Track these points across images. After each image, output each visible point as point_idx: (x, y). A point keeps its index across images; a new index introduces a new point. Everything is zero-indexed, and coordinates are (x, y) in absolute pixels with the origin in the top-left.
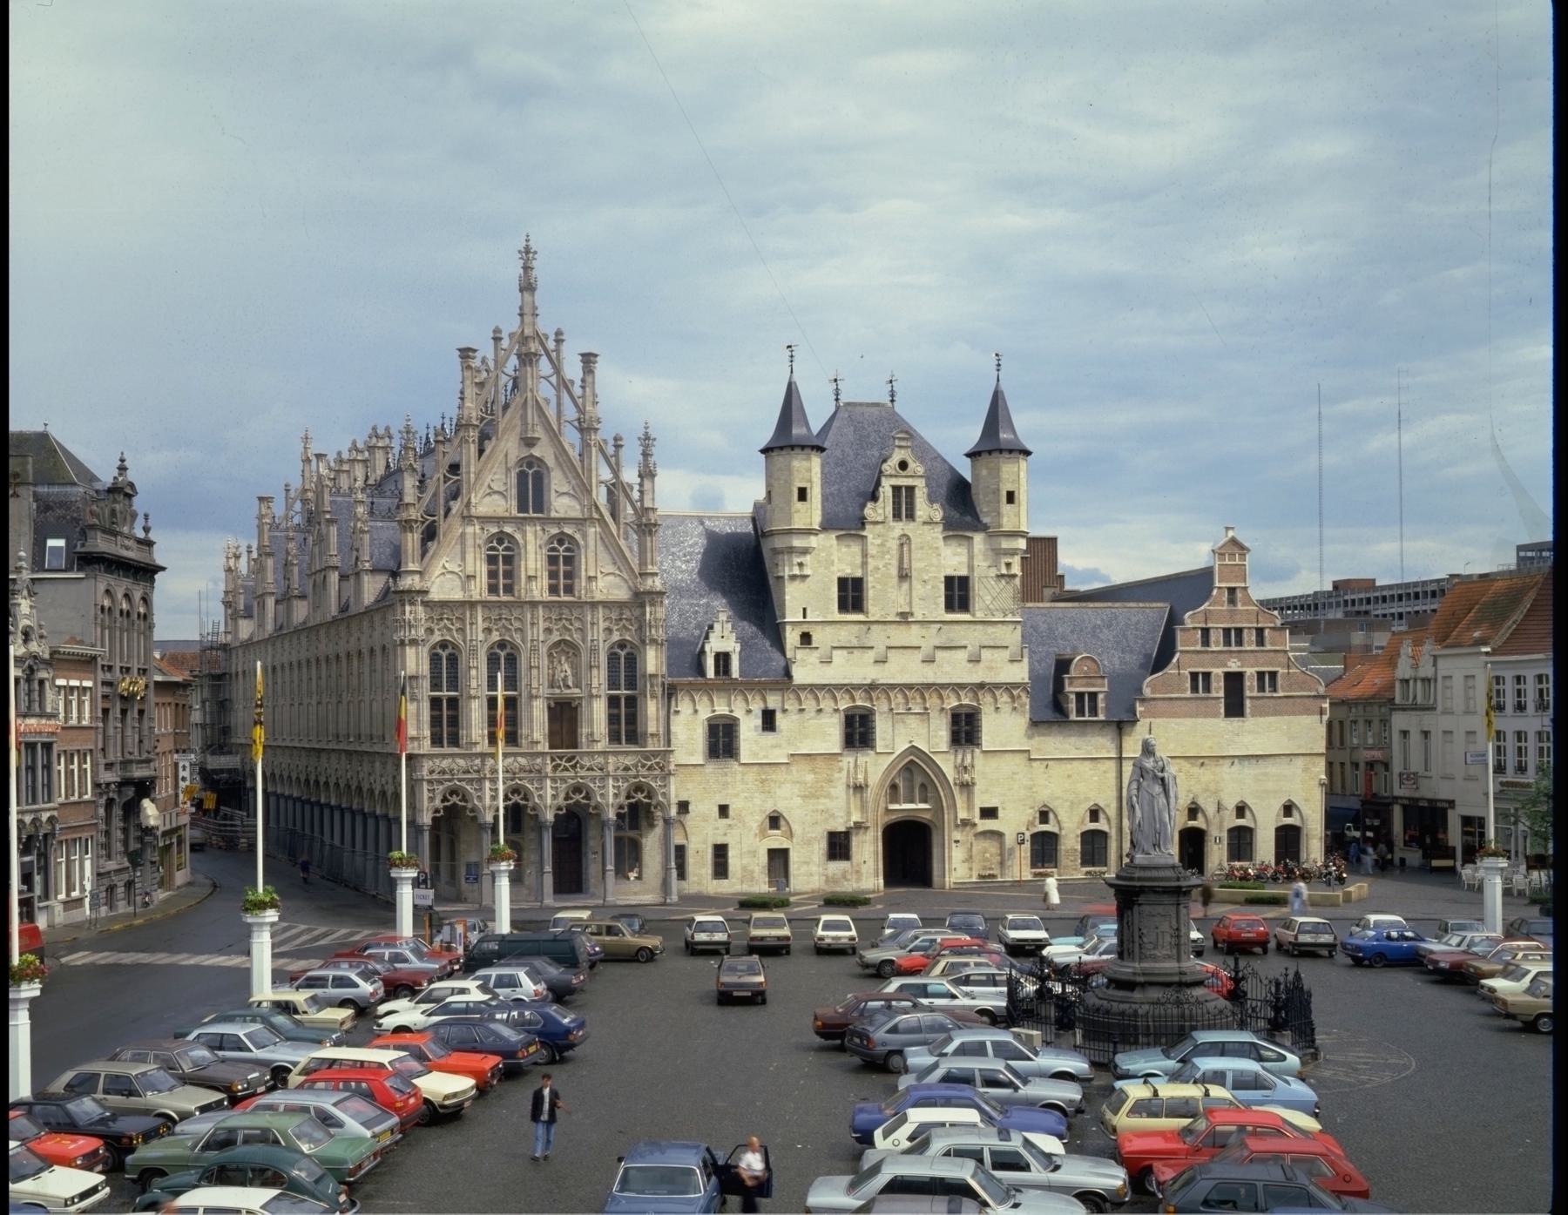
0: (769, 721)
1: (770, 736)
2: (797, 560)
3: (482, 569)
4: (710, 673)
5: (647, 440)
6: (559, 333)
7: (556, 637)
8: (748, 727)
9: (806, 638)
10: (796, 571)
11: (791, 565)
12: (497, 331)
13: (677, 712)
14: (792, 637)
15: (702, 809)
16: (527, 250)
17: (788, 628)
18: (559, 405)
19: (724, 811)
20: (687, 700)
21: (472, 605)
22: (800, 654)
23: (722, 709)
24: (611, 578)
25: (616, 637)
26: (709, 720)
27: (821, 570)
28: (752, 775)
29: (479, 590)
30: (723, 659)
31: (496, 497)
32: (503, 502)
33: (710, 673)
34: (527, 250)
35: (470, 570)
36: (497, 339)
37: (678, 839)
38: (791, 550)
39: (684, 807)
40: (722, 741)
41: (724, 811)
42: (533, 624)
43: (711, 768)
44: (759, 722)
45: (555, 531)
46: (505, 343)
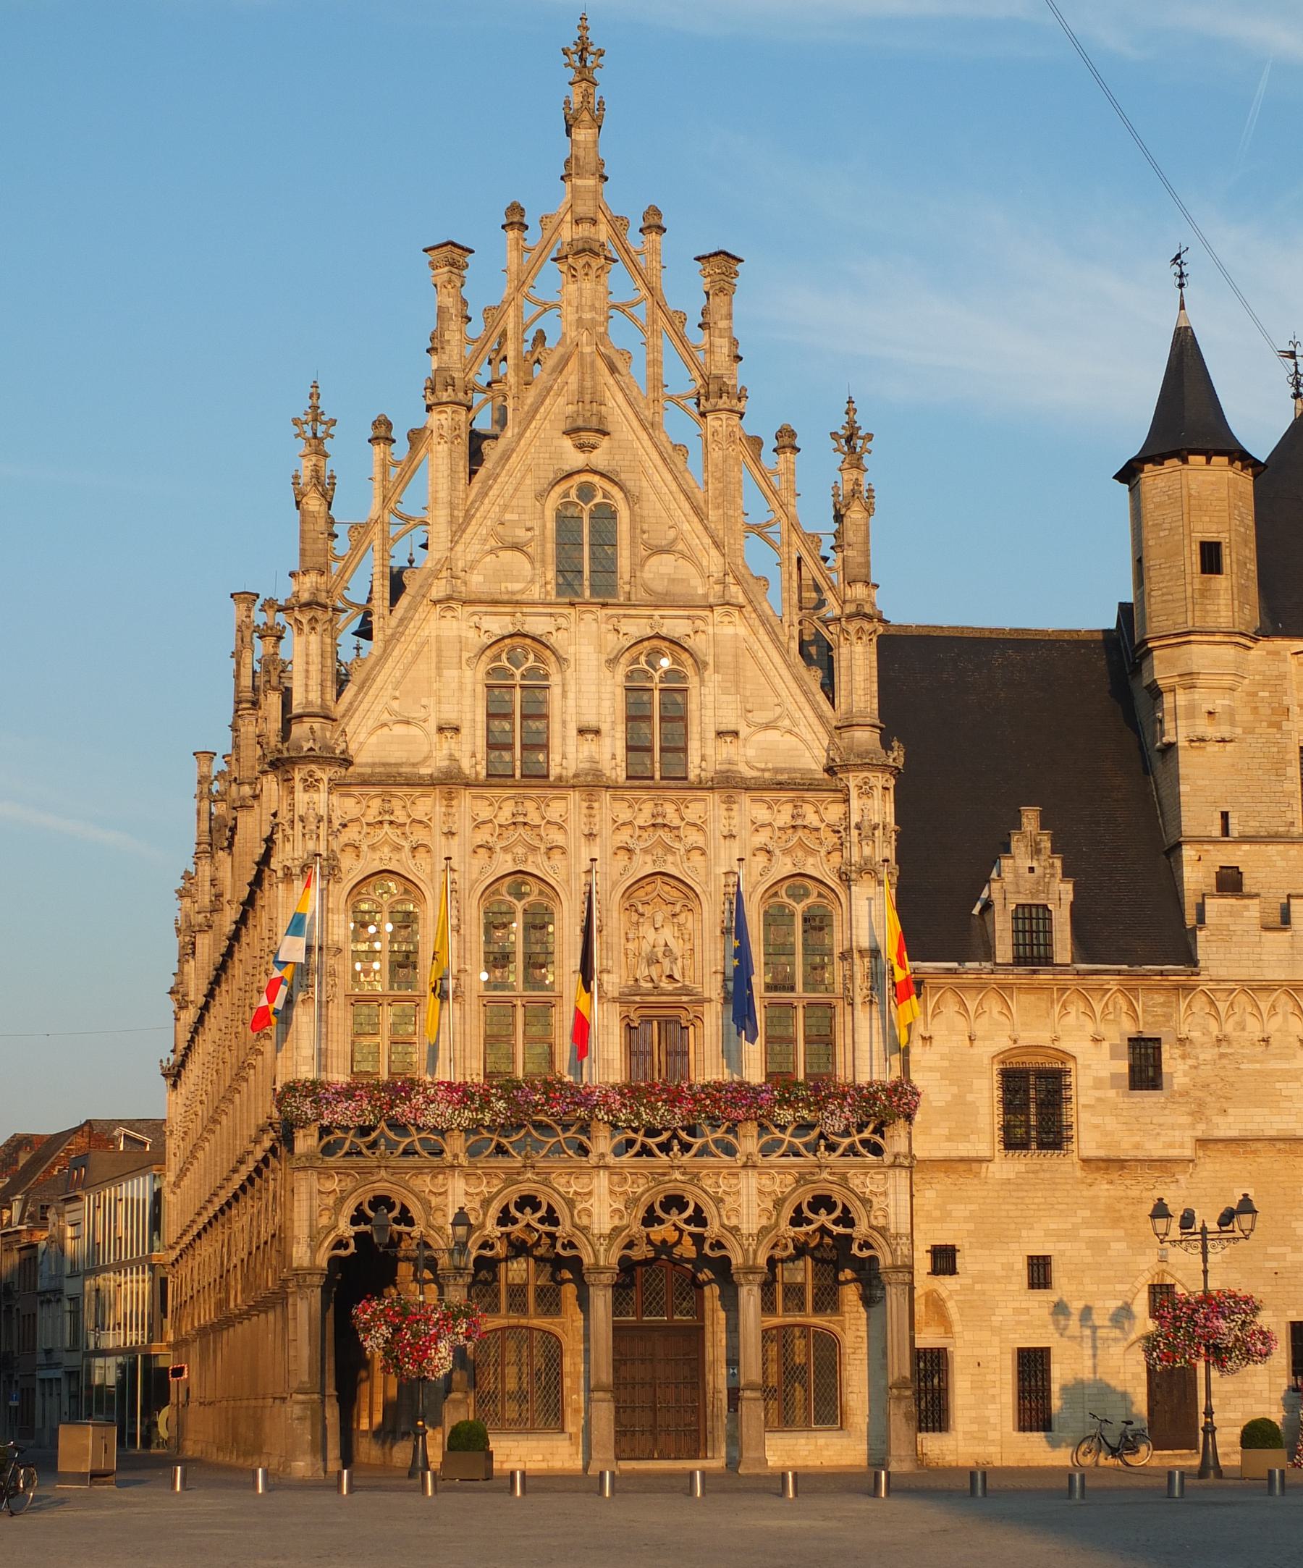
0: (1145, 1067)
1: (1148, 1098)
2: (1205, 699)
3: (473, 715)
4: (1004, 951)
5: (851, 441)
6: (654, 211)
7: (643, 865)
8: (1095, 1068)
9: (1230, 882)
10: (1204, 728)
11: (1191, 711)
12: (515, 209)
13: (927, 1039)
14: (1195, 873)
15: (992, 1268)
16: (583, 48)
17: (1188, 852)
18: (654, 363)
19: (1040, 1272)
20: (950, 1007)
21: (449, 782)
22: (1214, 907)
23: (1036, 1033)
24: (772, 735)
25: (784, 866)
26: (1003, 1056)
27: (1262, 728)
28: (1104, 1189)
29: (469, 752)
30: (1032, 921)
31: (507, 555)
32: (528, 566)
33: (1004, 951)
34: (583, 48)
35: (450, 715)
36: (515, 220)
37: (927, 1338)
38: (1189, 680)
39: (944, 1260)
40: (1034, 1104)
41: (1040, 1272)
42: (590, 836)
43: (1008, 1167)
44: (1123, 1066)
45: (636, 628)
46: (534, 236)
